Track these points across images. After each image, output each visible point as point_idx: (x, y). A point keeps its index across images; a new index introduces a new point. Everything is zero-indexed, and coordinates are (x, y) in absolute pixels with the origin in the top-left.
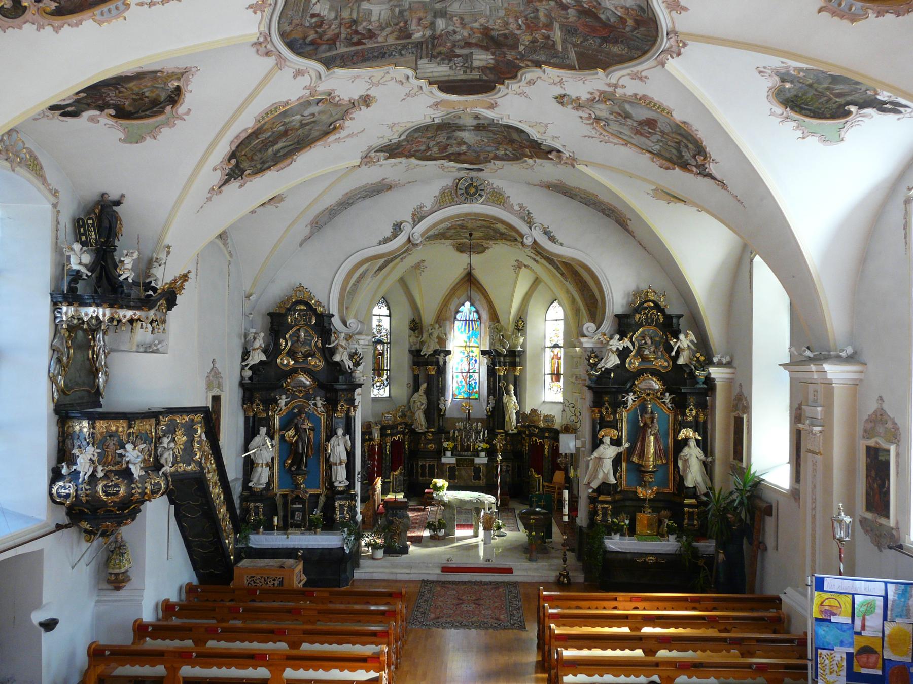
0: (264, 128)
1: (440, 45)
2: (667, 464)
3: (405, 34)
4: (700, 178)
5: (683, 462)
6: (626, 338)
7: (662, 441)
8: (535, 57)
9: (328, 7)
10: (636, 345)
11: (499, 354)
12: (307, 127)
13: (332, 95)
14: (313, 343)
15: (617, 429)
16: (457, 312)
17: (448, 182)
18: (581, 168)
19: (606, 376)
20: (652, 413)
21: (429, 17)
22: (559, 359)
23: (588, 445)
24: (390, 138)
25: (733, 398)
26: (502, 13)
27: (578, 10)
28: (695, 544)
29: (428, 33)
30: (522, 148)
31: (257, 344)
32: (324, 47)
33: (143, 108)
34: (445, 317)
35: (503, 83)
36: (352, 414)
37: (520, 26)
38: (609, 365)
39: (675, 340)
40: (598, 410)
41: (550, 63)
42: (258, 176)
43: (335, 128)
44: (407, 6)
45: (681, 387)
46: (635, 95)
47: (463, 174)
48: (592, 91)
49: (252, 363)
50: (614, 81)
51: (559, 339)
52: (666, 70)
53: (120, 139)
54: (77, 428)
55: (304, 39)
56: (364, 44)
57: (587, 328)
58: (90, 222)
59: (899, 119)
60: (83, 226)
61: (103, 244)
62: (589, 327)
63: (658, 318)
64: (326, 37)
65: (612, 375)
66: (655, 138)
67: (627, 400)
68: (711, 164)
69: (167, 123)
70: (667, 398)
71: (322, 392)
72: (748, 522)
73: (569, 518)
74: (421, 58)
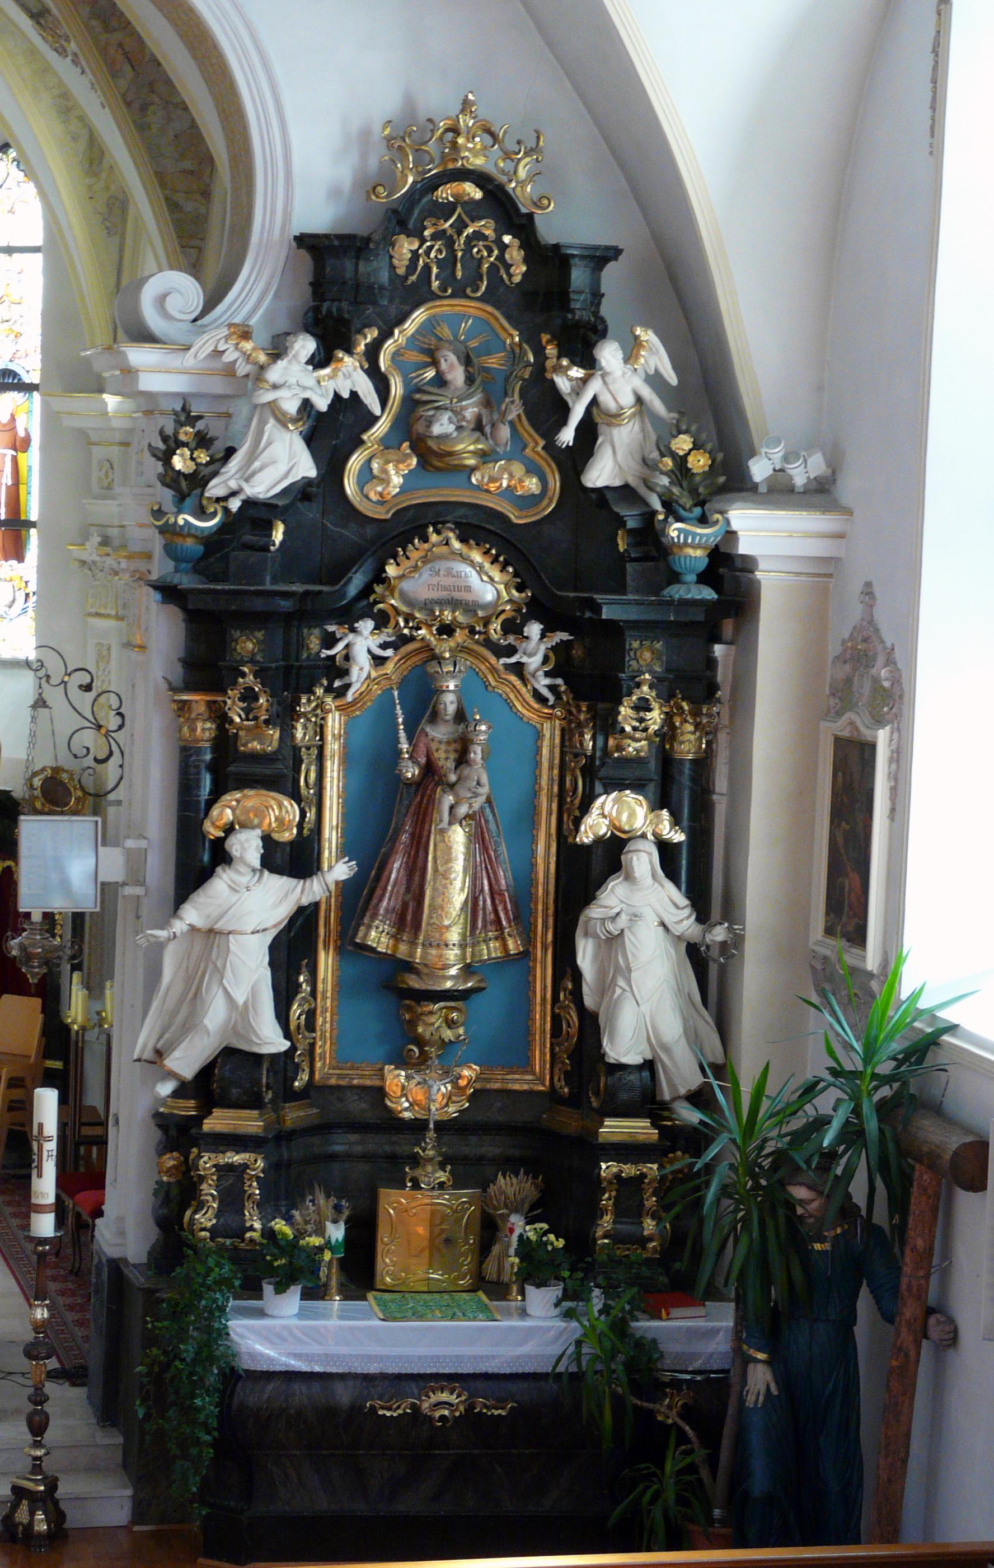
2: (526, 955)
5: (598, 947)
6: (349, 351)
7: (503, 848)
10: (397, 388)
15: (296, 796)
19: (248, 538)
20: (460, 716)
22: (21, 445)
25: (834, 649)
28: (644, 1326)
39: (577, 372)
40: (210, 704)
45: (598, 597)
51: (23, 344)
57: (161, 300)
63: (501, 258)
65: (278, 535)
67: (347, 658)
72: (881, 1216)
73: (59, 1223)
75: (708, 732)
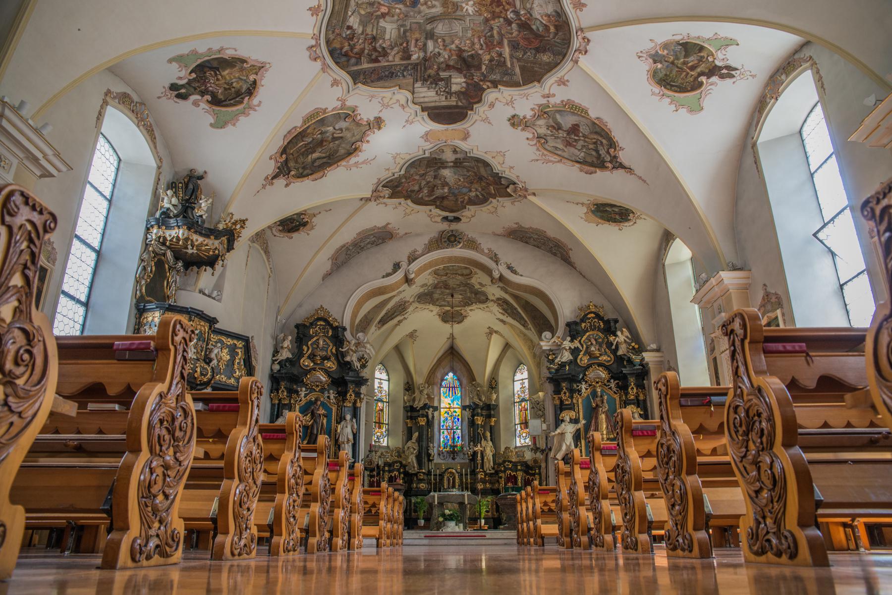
0: (308, 131)
1: (430, 68)
3: (407, 55)
4: (615, 172)
8: (493, 77)
9: (358, 20)
10: (585, 346)
11: (477, 406)
12: (336, 142)
13: (356, 113)
14: (330, 348)
16: (443, 380)
17: (434, 234)
18: (531, 198)
20: (601, 396)
21: (423, 39)
22: (526, 410)
23: (552, 426)
24: (394, 171)
26: (469, 34)
27: (517, 24)
29: (422, 55)
30: (488, 184)
31: (287, 344)
32: (353, 61)
33: (230, 98)
34: (433, 379)
35: (472, 110)
36: (358, 405)
37: (481, 45)
38: (564, 360)
41: (503, 81)
42: (299, 180)
43: (356, 149)
44: (408, 28)
46: (562, 101)
47: (445, 226)
48: (533, 106)
49: (281, 358)
50: (547, 92)
52: (579, 66)
53: (211, 125)
54: (150, 319)
55: (341, 49)
56: (379, 62)
57: (545, 337)
58: (180, 185)
59: (734, 83)
60: (175, 187)
61: (187, 201)
62: (547, 334)
64: (355, 51)
65: (567, 367)
66: (581, 143)
67: (581, 388)
68: (620, 152)
69: (244, 113)
70: (613, 384)
71: (335, 388)
74: (417, 81)
75: (645, 395)
